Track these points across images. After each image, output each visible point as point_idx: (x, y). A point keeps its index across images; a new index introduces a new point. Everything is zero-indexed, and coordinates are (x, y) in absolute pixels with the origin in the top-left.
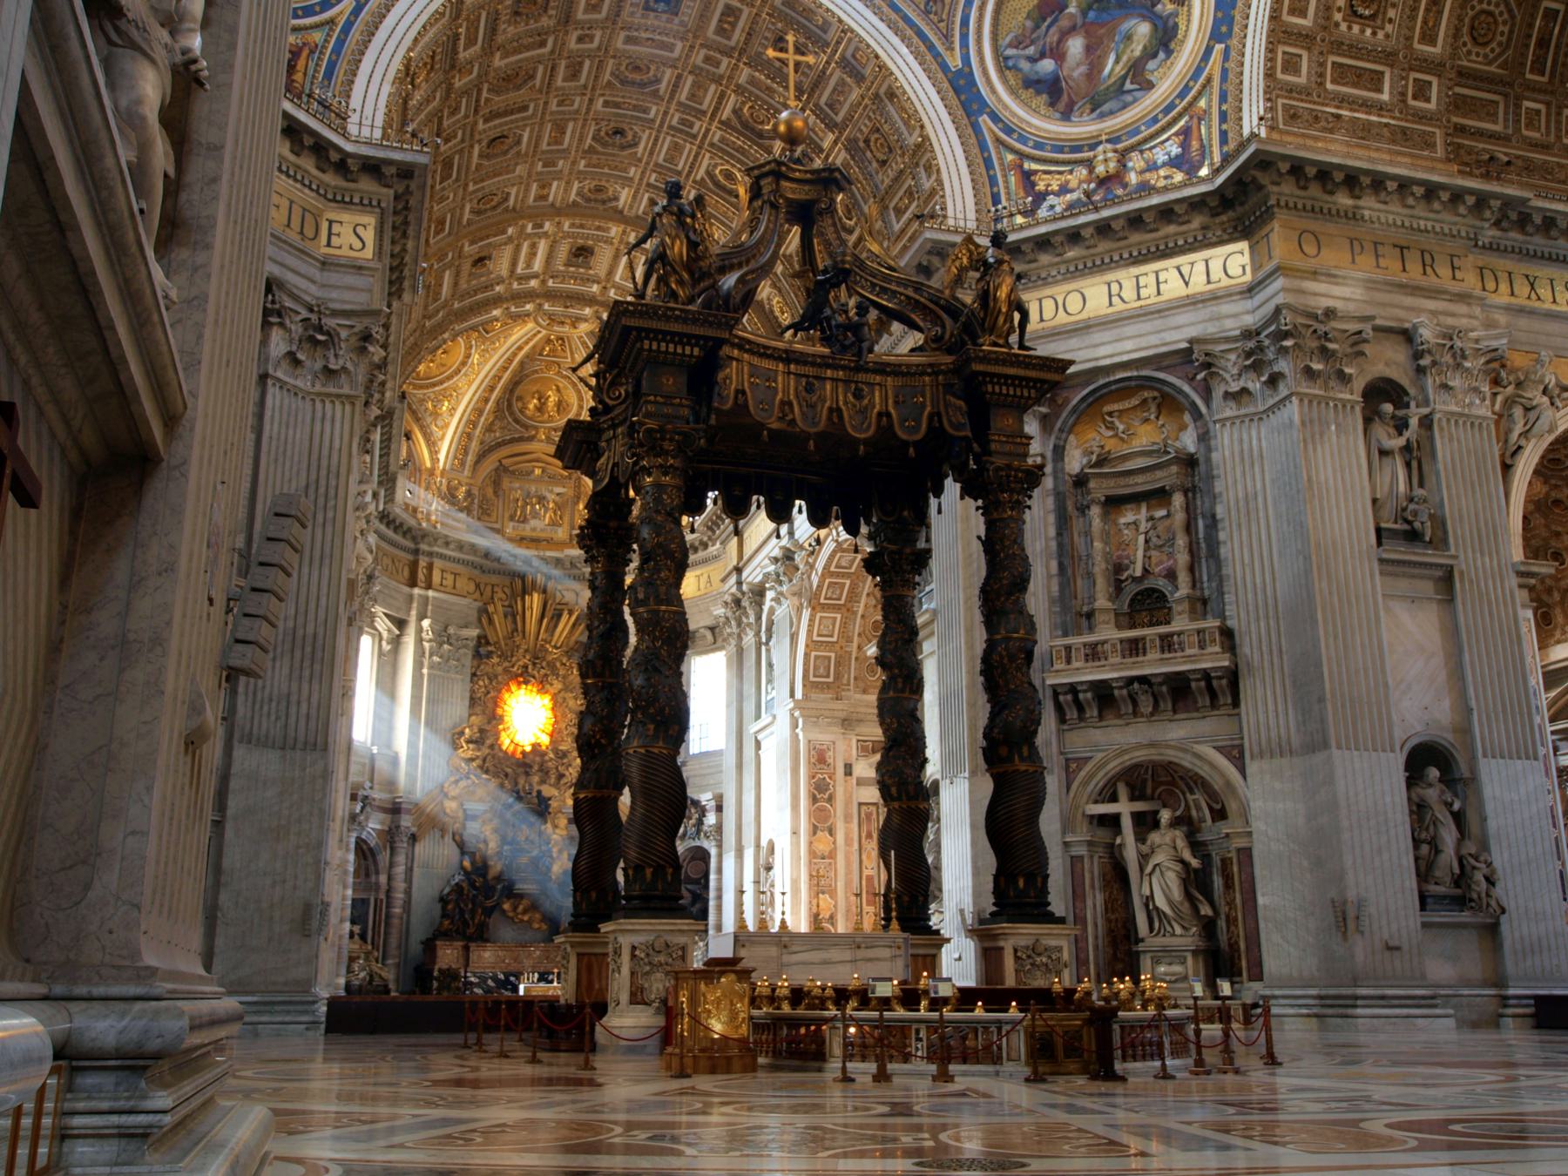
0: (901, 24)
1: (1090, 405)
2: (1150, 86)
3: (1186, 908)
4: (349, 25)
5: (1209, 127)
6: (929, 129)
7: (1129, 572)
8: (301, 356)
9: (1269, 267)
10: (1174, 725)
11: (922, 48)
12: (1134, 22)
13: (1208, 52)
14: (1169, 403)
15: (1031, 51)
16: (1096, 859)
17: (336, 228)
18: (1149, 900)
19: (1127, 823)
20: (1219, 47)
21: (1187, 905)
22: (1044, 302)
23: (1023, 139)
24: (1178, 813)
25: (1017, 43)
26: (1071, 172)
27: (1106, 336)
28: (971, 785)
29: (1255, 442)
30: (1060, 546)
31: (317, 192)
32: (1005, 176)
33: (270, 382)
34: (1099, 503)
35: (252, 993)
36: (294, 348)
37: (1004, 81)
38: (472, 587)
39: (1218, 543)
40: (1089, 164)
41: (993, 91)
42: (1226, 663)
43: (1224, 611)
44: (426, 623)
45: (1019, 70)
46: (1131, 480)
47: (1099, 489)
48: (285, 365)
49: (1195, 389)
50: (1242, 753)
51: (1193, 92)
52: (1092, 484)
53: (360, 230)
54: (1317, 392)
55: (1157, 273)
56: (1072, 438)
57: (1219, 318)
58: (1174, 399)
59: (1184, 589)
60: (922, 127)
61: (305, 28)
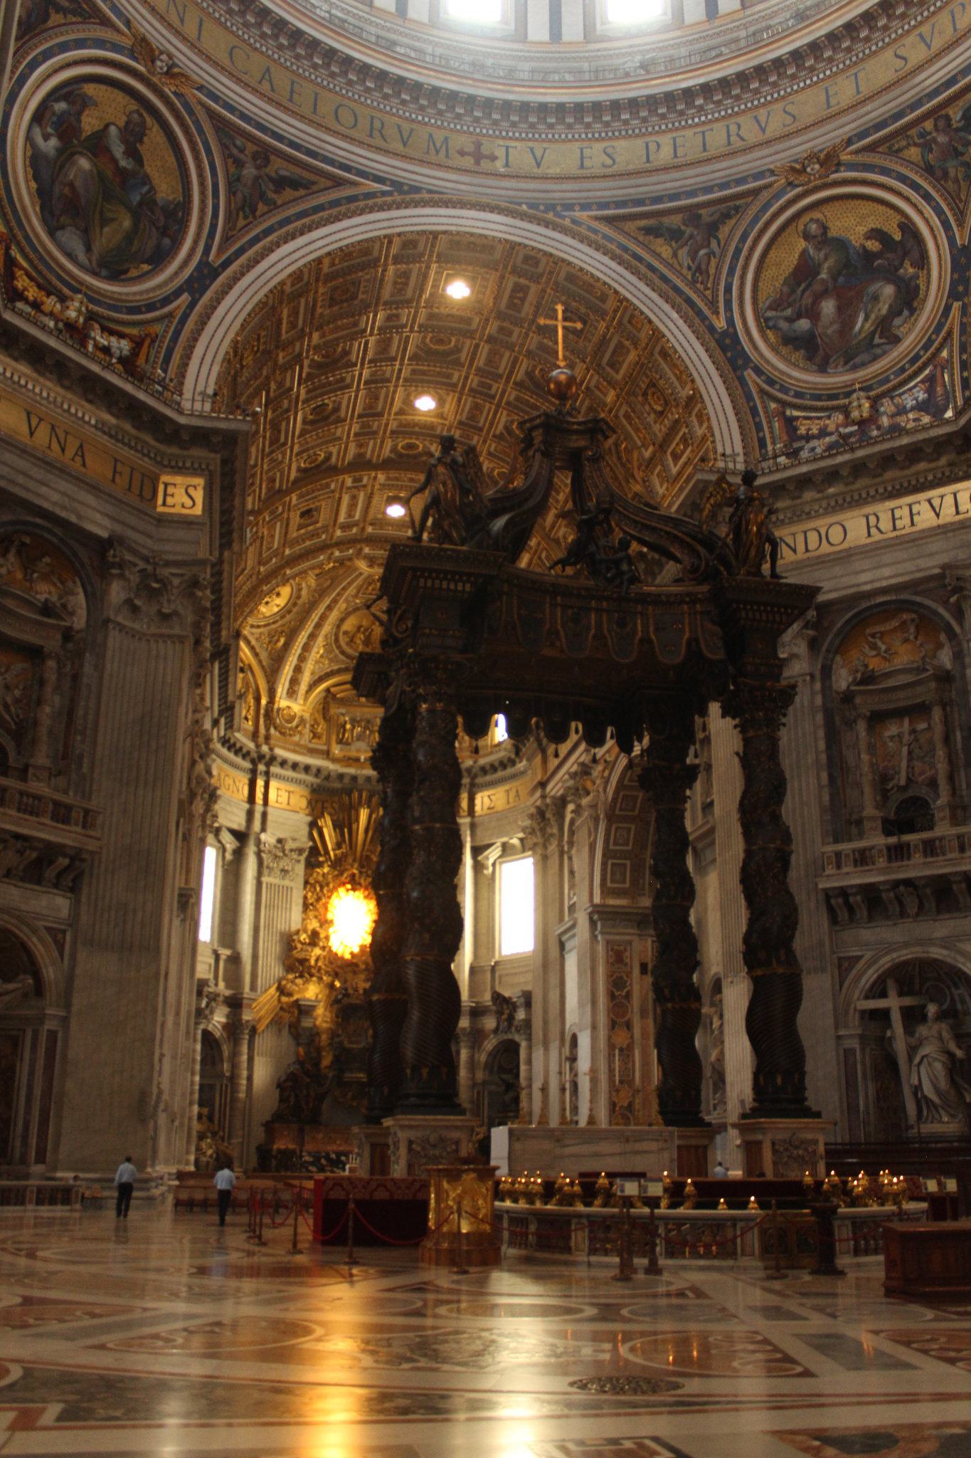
0: (671, 293)
2: (897, 340)
4: (185, 317)
5: (952, 376)
7: (895, 781)
8: (138, 602)
11: (691, 313)
12: (879, 285)
13: (948, 308)
14: (927, 624)
15: (789, 312)
16: (868, 1050)
17: (170, 490)
18: (917, 1089)
19: (896, 1017)
20: (957, 305)
22: (809, 534)
23: (784, 390)
24: (945, 1007)
25: (775, 306)
26: (829, 417)
30: (829, 758)
31: (154, 459)
32: (769, 422)
33: (111, 626)
35: (95, 1171)
36: (132, 595)
40: (845, 410)
41: (756, 348)
45: (780, 329)
47: (864, 705)
49: (948, 610)
51: (936, 344)
52: (858, 700)
53: (191, 491)
55: (910, 506)
56: (838, 658)
60: (693, 381)
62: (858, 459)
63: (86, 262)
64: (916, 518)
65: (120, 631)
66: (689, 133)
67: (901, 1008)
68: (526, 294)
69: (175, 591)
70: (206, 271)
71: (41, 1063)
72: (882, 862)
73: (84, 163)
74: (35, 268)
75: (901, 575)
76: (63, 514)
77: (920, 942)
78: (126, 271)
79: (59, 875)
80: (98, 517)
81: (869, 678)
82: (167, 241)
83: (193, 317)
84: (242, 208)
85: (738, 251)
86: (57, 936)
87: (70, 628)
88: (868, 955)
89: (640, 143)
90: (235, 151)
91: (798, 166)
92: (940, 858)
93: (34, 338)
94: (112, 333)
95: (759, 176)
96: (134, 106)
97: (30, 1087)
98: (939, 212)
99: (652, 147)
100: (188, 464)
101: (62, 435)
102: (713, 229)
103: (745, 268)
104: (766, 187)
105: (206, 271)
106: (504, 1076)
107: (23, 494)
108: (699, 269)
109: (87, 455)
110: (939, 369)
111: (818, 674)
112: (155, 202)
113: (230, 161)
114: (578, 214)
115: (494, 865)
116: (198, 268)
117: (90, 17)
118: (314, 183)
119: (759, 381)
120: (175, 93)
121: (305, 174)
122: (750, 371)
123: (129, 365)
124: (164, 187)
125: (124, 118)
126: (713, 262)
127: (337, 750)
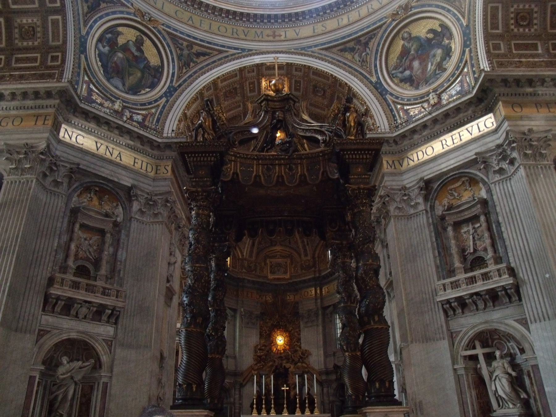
0: (353, 71)
1: (441, 188)
2: (445, 70)
3: (513, 395)
5: (470, 77)
7: (468, 251)
8: (144, 210)
9: (501, 119)
11: (362, 77)
15: (401, 69)
17: (159, 168)
20: (467, 50)
22: (418, 153)
23: (402, 99)
25: (396, 68)
27: (444, 160)
29: (510, 189)
30: (437, 244)
33: (133, 219)
37: (393, 82)
39: (502, 232)
40: (427, 101)
41: (389, 86)
42: (512, 282)
43: (509, 260)
47: (450, 220)
48: (139, 213)
50: (526, 321)
51: (461, 67)
53: (166, 167)
54: (531, 162)
55: (459, 133)
56: (437, 202)
57: (486, 144)
58: (474, 179)
59: (490, 254)
60: (365, 103)
61: (149, 109)
62: (433, 117)
63: (123, 90)
64: (462, 137)
65: (137, 221)
66: (353, 12)
67: (484, 354)
68: (300, 84)
69: (160, 205)
70: (172, 89)
72: (464, 286)
73: (120, 55)
74: (100, 91)
75: (459, 162)
76: (111, 178)
78: (140, 92)
80: (127, 179)
82: (156, 80)
84: (184, 65)
85: (377, 50)
86: (109, 343)
87: (116, 221)
89: (335, 20)
90: (180, 46)
91: (395, 12)
92: (491, 281)
94: (135, 113)
95: (380, 20)
96: (138, 33)
97: (95, 407)
98: (454, 15)
99: (340, 20)
100: (165, 158)
102: (366, 44)
103: (381, 56)
104: (384, 24)
105: (172, 89)
107: (94, 171)
108: (363, 61)
110: (464, 76)
111: (429, 209)
112: (150, 66)
113: (178, 49)
114: (313, 49)
116: (169, 88)
117: (117, 3)
118: (211, 53)
120: (154, 27)
121: (208, 51)
123: (142, 124)
124: (153, 61)
125: (135, 38)
126: (368, 57)
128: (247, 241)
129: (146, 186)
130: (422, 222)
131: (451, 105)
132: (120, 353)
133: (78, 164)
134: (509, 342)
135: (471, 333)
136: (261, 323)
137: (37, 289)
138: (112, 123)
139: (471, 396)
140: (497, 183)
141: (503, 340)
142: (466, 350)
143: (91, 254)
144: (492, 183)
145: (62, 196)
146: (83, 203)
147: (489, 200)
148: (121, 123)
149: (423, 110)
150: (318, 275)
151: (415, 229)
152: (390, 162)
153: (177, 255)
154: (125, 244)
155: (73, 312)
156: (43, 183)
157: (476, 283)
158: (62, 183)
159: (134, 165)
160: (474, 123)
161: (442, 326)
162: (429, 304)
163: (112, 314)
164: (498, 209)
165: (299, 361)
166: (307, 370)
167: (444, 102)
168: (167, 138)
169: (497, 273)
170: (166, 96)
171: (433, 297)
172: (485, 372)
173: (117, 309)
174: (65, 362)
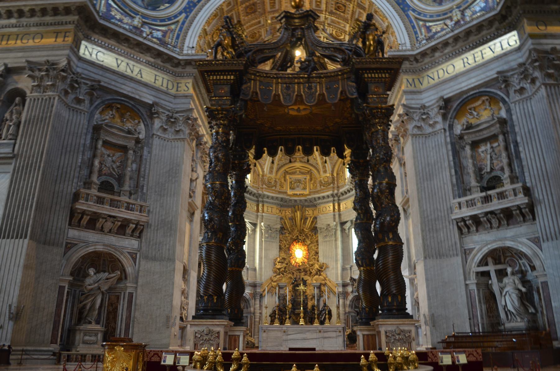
3: (522, 310)
6: (389, 19)
7: (485, 170)
8: (166, 127)
10: (508, 231)
14: (493, 99)
17: (180, 85)
21: (522, 308)
23: (425, 16)
27: (464, 78)
28: (425, 263)
29: (530, 108)
30: (455, 163)
33: (155, 136)
34: (469, 144)
38: (278, 211)
42: (527, 201)
43: (525, 179)
44: (262, 224)
46: (481, 133)
47: (469, 139)
48: (160, 131)
50: (539, 240)
52: (465, 137)
53: (187, 84)
55: (481, 51)
56: (456, 121)
58: (495, 98)
59: (507, 173)
60: (387, 19)
63: (142, 5)
64: (484, 56)
67: (496, 271)
69: (181, 122)
70: (191, 4)
71: (126, 305)
72: (479, 205)
76: (133, 95)
77: (500, 240)
78: (159, 7)
79: (133, 231)
80: (148, 96)
81: (469, 127)
83: (187, 21)
87: (138, 138)
88: (477, 247)
92: (506, 200)
93: (114, 30)
94: (154, 29)
101: (131, 67)
106: (356, 310)
109: (143, 73)
111: (447, 128)
115: (349, 229)
119: (414, 14)
122: (411, 11)
127: (290, 192)
128: (267, 159)
129: (168, 104)
130: (439, 140)
131: (475, 22)
132: (145, 265)
133: (99, 81)
134: (521, 259)
135: (485, 250)
136: (281, 236)
137: (63, 204)
138: (131, 39)
139: (481, 310)
140: (517, 103)
141: (515, 258)
142: (478, 266)
143: (115, 171)
144: (512, 103)
145: (84, 114)
146: (105, 120)
147: (508, 119)
148: (141, 39)
149: (445, 27)
150: (336, 192)
151: (433, 148)
152: (411, 81)
153: (198, 172)
154: (148, 160)
155: (98, 225)
156: (65, 99)
157: (491, 201)
158: (84, 100)
159: (155, 83)
160: (497, 41)
161: (456, 243)
162: (444, 221)
163: (136, 228)
164: (517, 129)
165: (317, 274)
166: (323, 282)
167: (468, 19)
168: (187, 55)
169: (512, 193)
170: (186, 12)
171: (448, 214)
172: (496, 288)
173: (141, 223)
174: (92, 273)
